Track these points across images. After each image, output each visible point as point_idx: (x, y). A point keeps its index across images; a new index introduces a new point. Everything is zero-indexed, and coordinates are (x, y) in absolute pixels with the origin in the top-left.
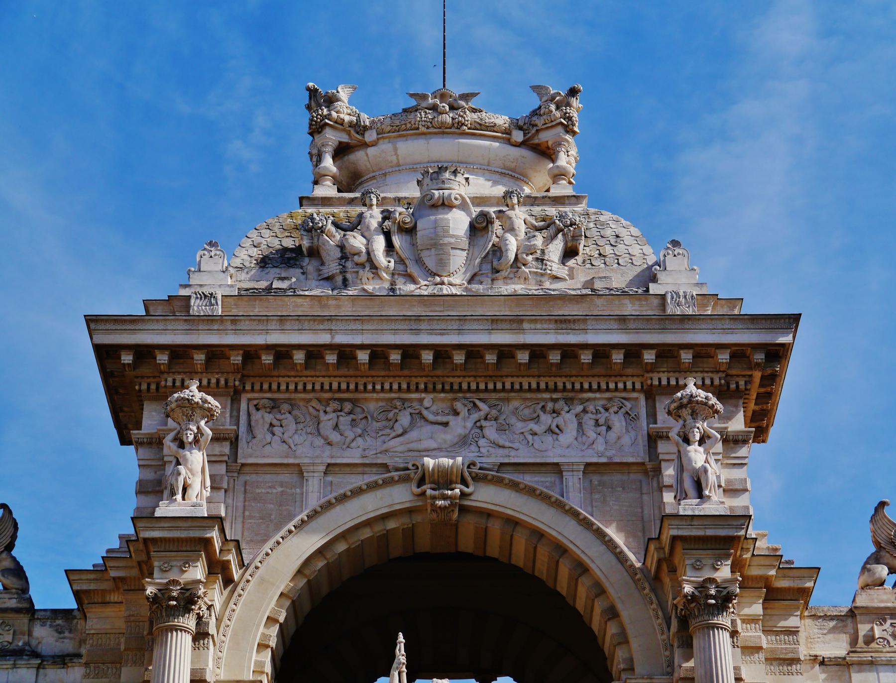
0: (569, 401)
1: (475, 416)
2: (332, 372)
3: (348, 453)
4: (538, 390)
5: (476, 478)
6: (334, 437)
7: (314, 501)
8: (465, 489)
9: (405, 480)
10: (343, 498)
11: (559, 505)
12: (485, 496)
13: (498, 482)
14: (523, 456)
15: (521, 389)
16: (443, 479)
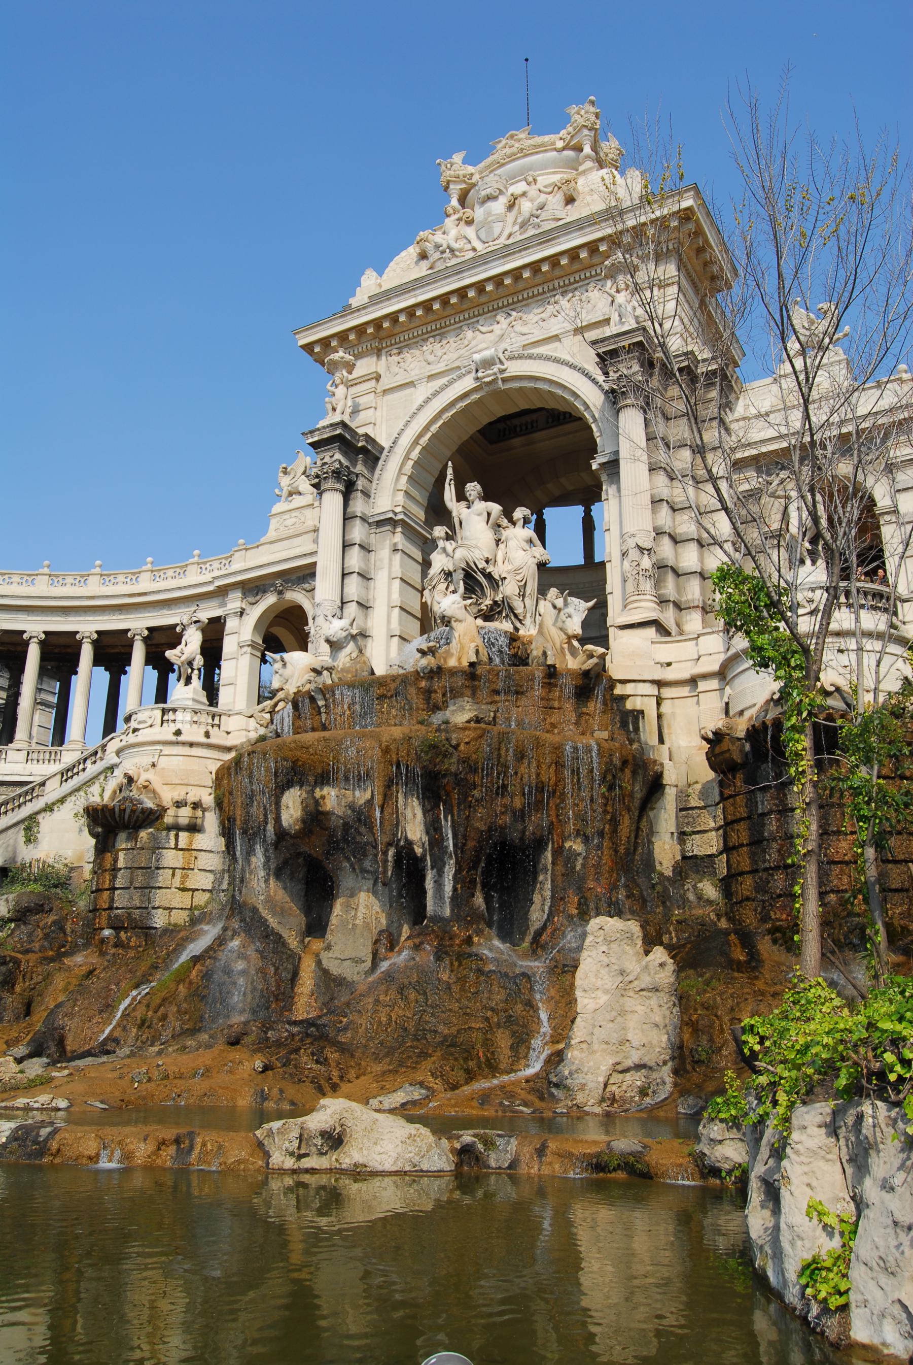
0: (564, 294)
1: (508, 320)
2: (424, 320)
3: (440, 365)
4: (544, 293)
5: (511, 358)
6: (431, 358)
7: (420, 400)
8: (503, 367)
9: (470, 372)
10: (436, 394)
11: (557, 361)
12: (515, 368)
13: (520, 357)
14: (538, 335)
15: (534, 296)
16: (487, 363)
